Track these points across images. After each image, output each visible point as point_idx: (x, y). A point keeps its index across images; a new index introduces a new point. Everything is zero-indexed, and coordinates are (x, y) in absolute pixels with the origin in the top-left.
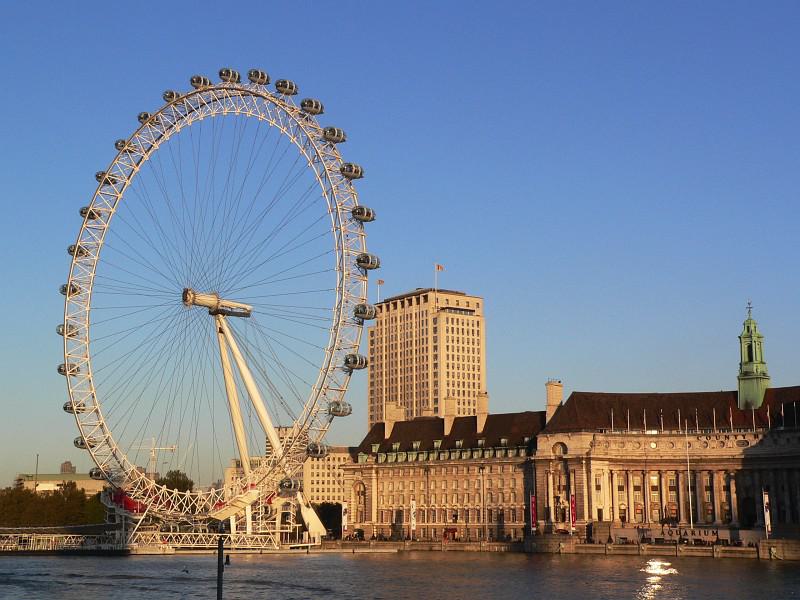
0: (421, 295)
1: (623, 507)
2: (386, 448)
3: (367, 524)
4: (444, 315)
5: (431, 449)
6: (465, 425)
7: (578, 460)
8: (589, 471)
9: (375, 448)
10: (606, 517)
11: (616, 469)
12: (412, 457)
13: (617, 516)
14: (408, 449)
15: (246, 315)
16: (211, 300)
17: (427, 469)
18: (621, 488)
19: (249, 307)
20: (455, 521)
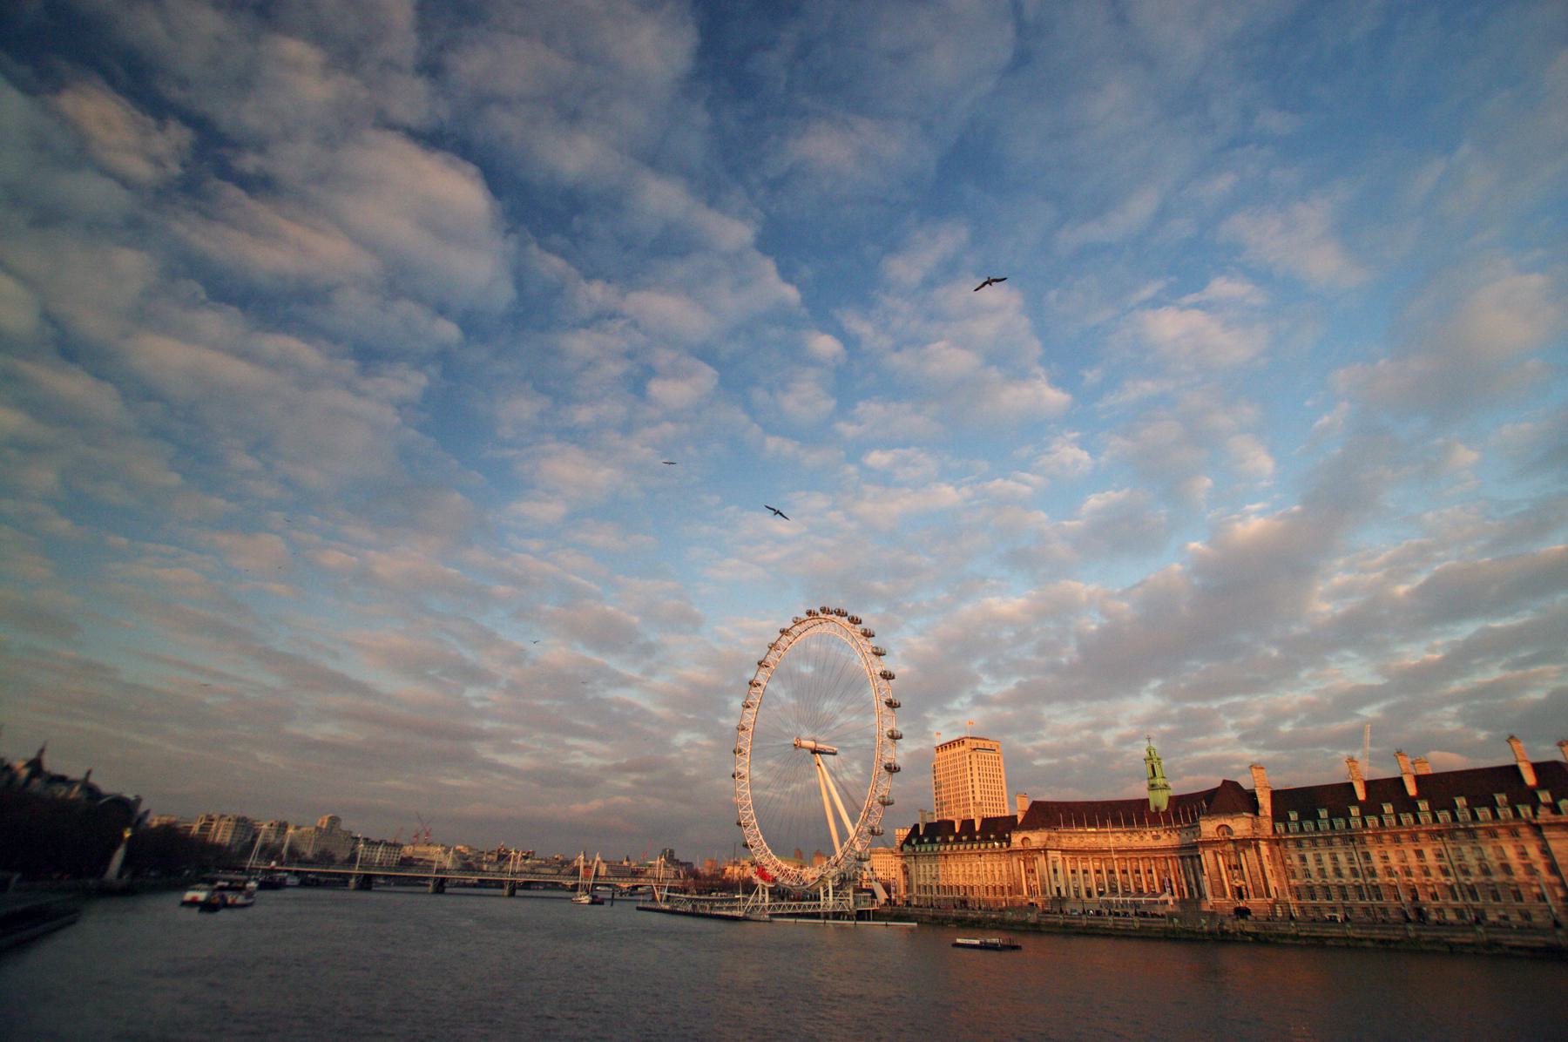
0: (960, 742)
2: (920, 842)
5: (948, 842)
6: (968, 824)
7: (1038, 850)
10: (1063, 893)
11: (1067, 857)
14: (932, 841)
16: (811, 744)
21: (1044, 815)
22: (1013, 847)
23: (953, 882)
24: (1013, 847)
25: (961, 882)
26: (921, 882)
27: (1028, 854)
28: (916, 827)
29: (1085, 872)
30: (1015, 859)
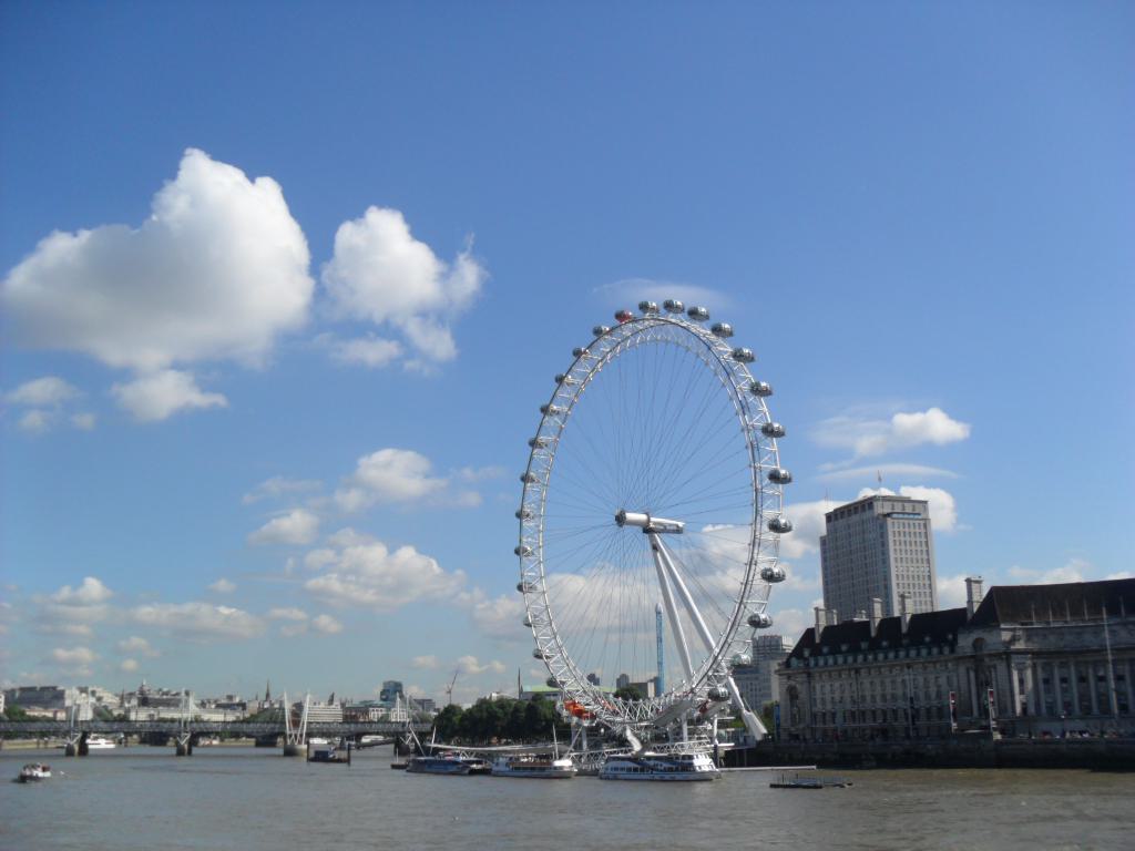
0: (868, 504)
1: (1050, 700)
2: (816, 652)
3: (801, 726)
4: (889, 520)
7: (998, 656)
8: (1009, 666)
9: (806, 653)
11: (1039, 662)
12: (840, 660)
13: (1044, 710)
14: (835, 651)
15: (678, 531)
17: (857, 671)
18: (1046, 681)
19: (681, 524)
20: (885, 720)
21: (1005, 603)
22: (959, 652)
23: (868, 705)
24: (959, 652)
25: (879, 704)
26: (819, 708)
27: (979, 662)
28: (810, 633)
29: (1064, 680)
30: (962, 670)
